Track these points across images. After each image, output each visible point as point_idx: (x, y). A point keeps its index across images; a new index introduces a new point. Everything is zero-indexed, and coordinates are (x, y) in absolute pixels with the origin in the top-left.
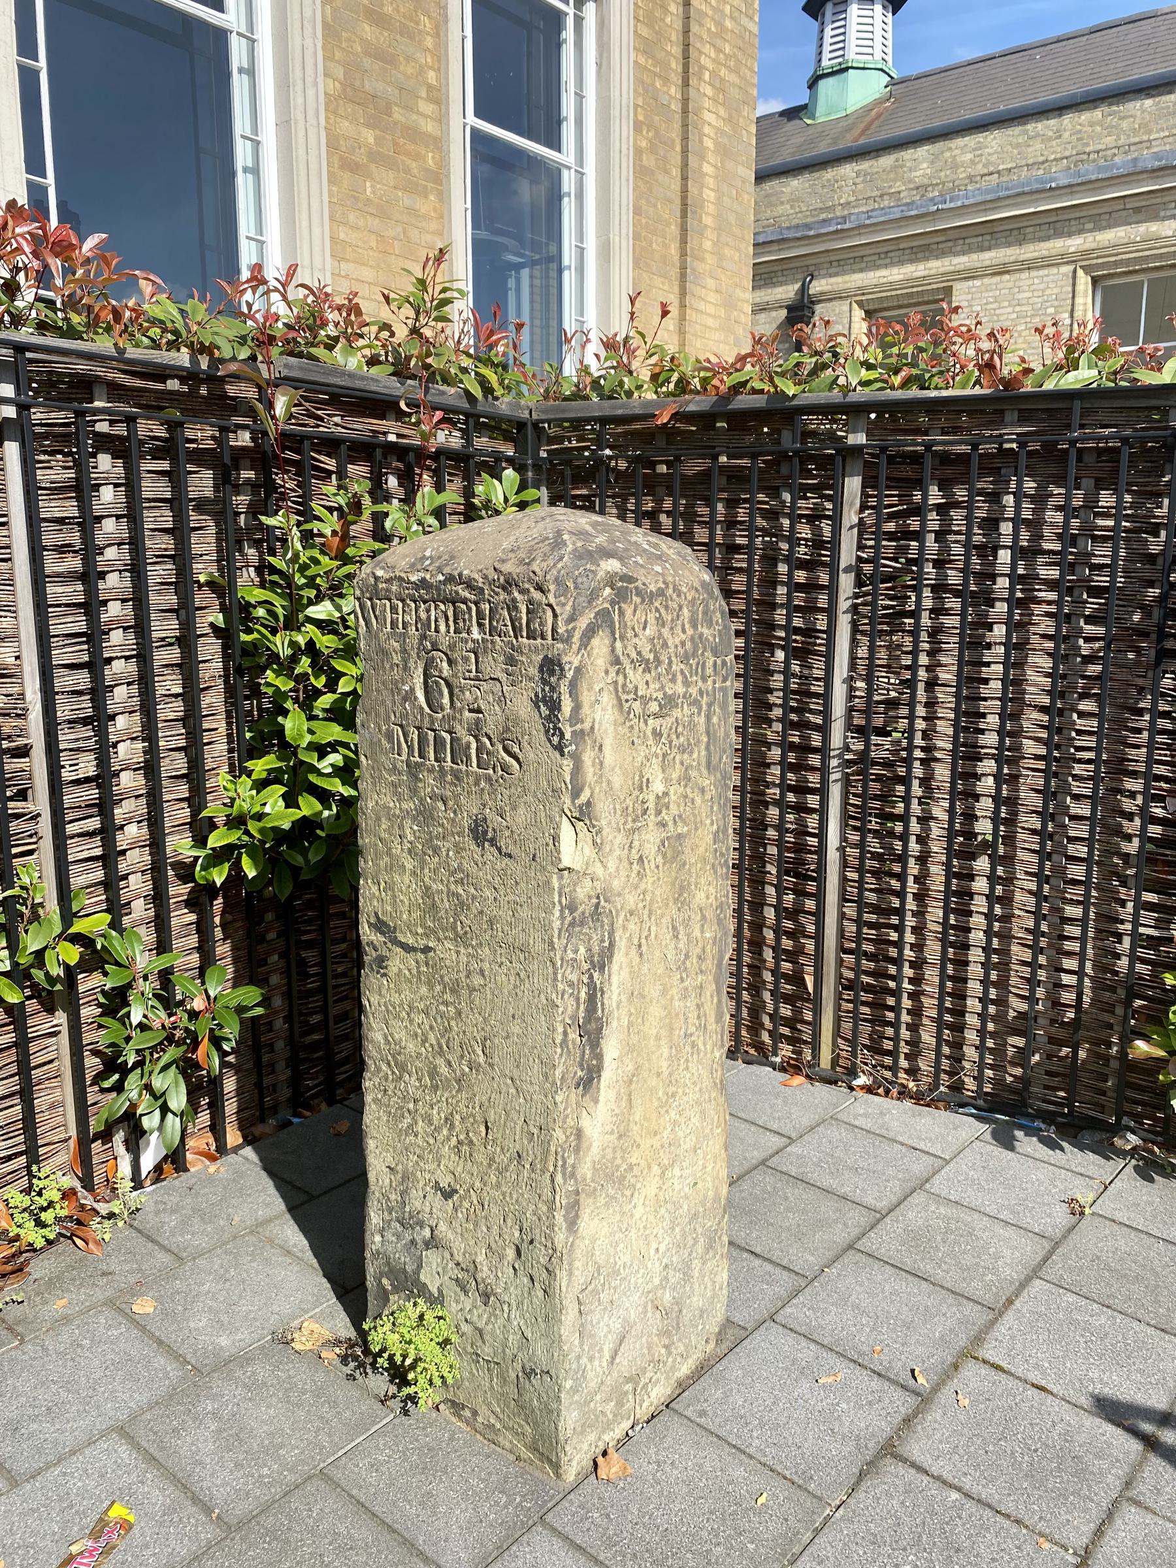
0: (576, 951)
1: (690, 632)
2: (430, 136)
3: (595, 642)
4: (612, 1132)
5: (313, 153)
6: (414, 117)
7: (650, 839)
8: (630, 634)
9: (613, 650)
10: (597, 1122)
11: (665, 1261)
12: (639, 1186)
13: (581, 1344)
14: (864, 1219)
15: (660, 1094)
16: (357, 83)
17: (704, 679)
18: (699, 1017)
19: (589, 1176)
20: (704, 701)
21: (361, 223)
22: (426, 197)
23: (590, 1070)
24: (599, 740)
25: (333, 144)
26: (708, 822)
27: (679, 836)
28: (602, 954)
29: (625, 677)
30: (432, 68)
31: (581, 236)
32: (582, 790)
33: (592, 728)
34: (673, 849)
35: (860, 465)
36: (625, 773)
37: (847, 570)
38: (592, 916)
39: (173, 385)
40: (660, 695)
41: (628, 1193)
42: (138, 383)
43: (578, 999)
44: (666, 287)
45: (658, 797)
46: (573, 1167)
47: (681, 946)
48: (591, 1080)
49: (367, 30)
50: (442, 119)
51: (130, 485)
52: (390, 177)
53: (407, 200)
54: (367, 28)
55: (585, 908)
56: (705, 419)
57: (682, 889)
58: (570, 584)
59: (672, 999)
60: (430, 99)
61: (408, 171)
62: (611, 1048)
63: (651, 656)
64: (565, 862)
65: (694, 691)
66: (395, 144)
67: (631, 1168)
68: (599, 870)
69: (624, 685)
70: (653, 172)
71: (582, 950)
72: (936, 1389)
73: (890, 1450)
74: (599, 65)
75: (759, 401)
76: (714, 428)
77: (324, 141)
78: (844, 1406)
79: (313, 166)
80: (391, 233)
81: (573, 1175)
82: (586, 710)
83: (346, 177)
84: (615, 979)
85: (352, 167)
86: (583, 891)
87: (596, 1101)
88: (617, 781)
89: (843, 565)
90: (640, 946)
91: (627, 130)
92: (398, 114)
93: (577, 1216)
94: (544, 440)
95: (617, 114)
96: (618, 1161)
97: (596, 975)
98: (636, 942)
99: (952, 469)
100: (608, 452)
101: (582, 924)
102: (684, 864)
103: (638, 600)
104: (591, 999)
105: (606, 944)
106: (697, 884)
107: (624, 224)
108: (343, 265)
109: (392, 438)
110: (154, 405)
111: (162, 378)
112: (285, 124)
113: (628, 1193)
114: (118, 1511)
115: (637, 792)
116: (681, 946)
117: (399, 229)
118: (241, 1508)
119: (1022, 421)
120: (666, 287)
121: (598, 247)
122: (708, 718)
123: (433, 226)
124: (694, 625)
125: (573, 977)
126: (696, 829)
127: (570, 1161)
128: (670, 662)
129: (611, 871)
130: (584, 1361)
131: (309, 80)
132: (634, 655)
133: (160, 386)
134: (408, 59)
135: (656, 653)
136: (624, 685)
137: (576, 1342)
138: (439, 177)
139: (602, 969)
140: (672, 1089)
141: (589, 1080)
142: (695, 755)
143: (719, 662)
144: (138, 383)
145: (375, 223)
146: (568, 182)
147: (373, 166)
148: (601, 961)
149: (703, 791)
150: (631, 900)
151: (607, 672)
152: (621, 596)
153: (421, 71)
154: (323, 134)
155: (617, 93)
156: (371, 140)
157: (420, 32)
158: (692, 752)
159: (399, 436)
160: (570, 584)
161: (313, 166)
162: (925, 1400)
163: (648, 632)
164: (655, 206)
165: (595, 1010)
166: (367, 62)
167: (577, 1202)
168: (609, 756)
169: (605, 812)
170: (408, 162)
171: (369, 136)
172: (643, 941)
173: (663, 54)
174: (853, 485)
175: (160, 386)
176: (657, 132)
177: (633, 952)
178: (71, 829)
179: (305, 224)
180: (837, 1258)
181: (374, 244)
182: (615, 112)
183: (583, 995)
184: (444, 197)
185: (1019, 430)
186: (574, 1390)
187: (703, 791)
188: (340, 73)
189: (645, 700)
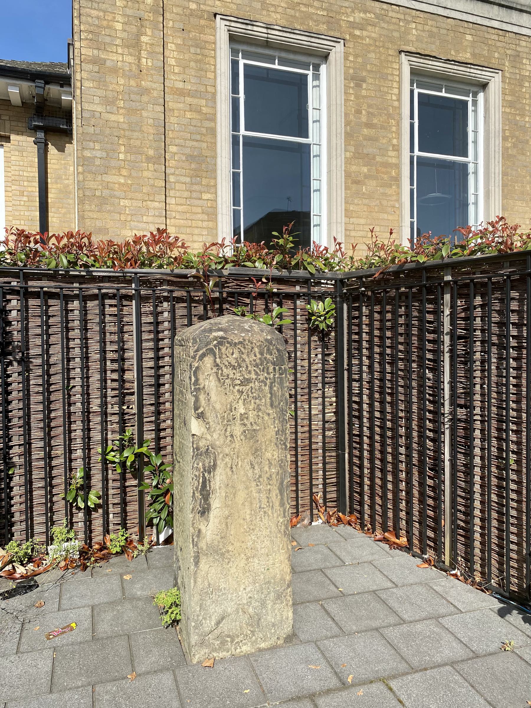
0: (198, 464)
1: (259, 356)
2: (394, 164)
3: (206, 359)
4: (217, 535)
5: (339, 181)
6: (386, 158)
7: (238, 430)
8: (224, 356)
9: (215, 362)
10: (210, 529)
11: (249, 595)
12: (232, 560)
13: (200, 611)
14: (392, 619)
15: (245, 527)
16: (360, 151)
17: (268, 373)
18: (268, 502)
19: (204, 548)
20: (268, 382)
21: (360, 202)
22: (391, 187)
23: (204, 508)
24: (207, 392)
25: (348, 175)
26: (272, 427)
27: (254, 430)
28: (210, 467)
29: (222, 371)
30: (395, 138)
31: (476, 189)
32: (199, 408)
33: (204, 387)
34: (251, 435)
35: (449, 289)
36: (222, 404)
37: (447, 334)
38: (205, 453)
39: (191, 279)
40: (241, 378)
41: (226, 561)
42: (179, 280)
43: (199, 482)
44: (524, 205)
45: (241, 414)
46: (197, 542)
47: (256, 471)
48: (204, 512)
49: (365, 131)
50: (399, 157)
51: (173, 311)
52: (373, 183)
53: (382, 190)
54: (365, 130)
55: (203, 450)
56: (396, 273)
57: (257, 450)
58: (198, 340)
59: (251, 491)
60: (393, 150)
61: (382, 179)
62: (215, 503)
63: (236, 364)
64: (193, 433)
65: (261, 377)
66: (377, 170)
67: (228, 551)
68: (209, 437)
69: (222, 374)
70: (515, 156)
71: (201, 464)
72: (353, 685)
73: (312, 697)
74: (485, 117)
75: (413, 265)
76: (400, 277)
77: (343, 176)
78: (310, 677)
79: (339, 185)
80: (374, 204)
81: (196, 545)
82: (201, 381)
83: (354, 187)
84: (217, 478)
85: (357, 182)
86: (202, 444)
87: (208, 521)
88: (218, 406)
89: (445, 332)
90: (232, 468)
91: (499, 141)
92: (378, 159)
93: (198, 561)
94: (345, 286)
95: (493, 136)
96: (221, 547)
97: (206, 475)
98: (229, 466)
99: (482, 289)
100: (363, 289)
101: (201, 455)
102: (258, 441)
103: (228, 345)
104: (204, 482)
105: (212, 464)
106: (266, 450)
107: (497, 181)
108: (351, 219)
109: (275, 290)
110: (181, 286)
111: (188, 278)
112: (329, 172)
113: (226, 561)
114: (74, 625)
115: (228, 412)
116: (256, 471)
117: (378, 202)
118: (101, 635)
119: (511, 266)
120: (524, 205)
121: (484, 192)
122: (271, 388)
123: (394, 198)
124: (261, 353)
125: (197, 474)
126: (265, 428)
127: (195, 540)
128: (247, 367)
129: (216, 437)
130: (201, 618)
131: (338, 155)
132: (227, 364)
133: (187, 280)
134: (383, 137)
135: (238, 363)
136: (222, 374)
137: (198, 610)
138: (397, 179)
139: (209, 473)
140: (252, 527)
141: (205, 511)
142: (263, 401)
143: (277, 368)
144: (179, 280)
145: (366, 201)
146: (471, 168)
147: (366, 180)
148: (212, 469)
149: (269, 414)
150: (227, 450)
151: (212, 369)
152: (220, 343)
153: (390, 140)
154: (343, 173)
155: (493, 127)
156: (366, 170)
157: (390, 126)
158: (261, 400)
159: (278, 289)
160: (198, 340)
161: (339, 185)
162: (344, 686)
163: (234, 356)
164: (517, 170)
165: (206, 487)
166: (365, 143)
167: (198, 556)
168: (214, 397)
169: (211, 417)
170: (383, 175)
171: (365, 170)
172: (234, 467)
173: (521, 105)
174: (447, 297)
175: (187, 280)
176: (517, 138)
177: (228, 470)
178: (145, 420)
179: (335, 207)
180: (366, 631)
181: (366, 210)
182: (492, 135)
183: (201, 480)
184: (399, 186)
185: (509, 270)
186: (196, 628)
187: (269, 414)
188: (352, 149)
189: (233, 380)
